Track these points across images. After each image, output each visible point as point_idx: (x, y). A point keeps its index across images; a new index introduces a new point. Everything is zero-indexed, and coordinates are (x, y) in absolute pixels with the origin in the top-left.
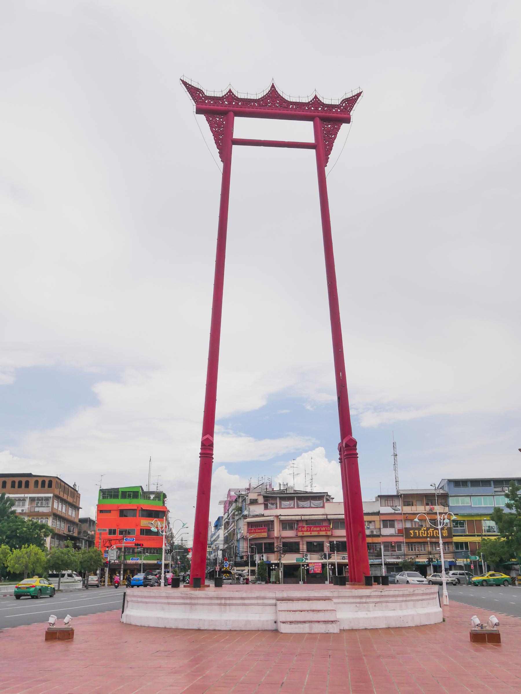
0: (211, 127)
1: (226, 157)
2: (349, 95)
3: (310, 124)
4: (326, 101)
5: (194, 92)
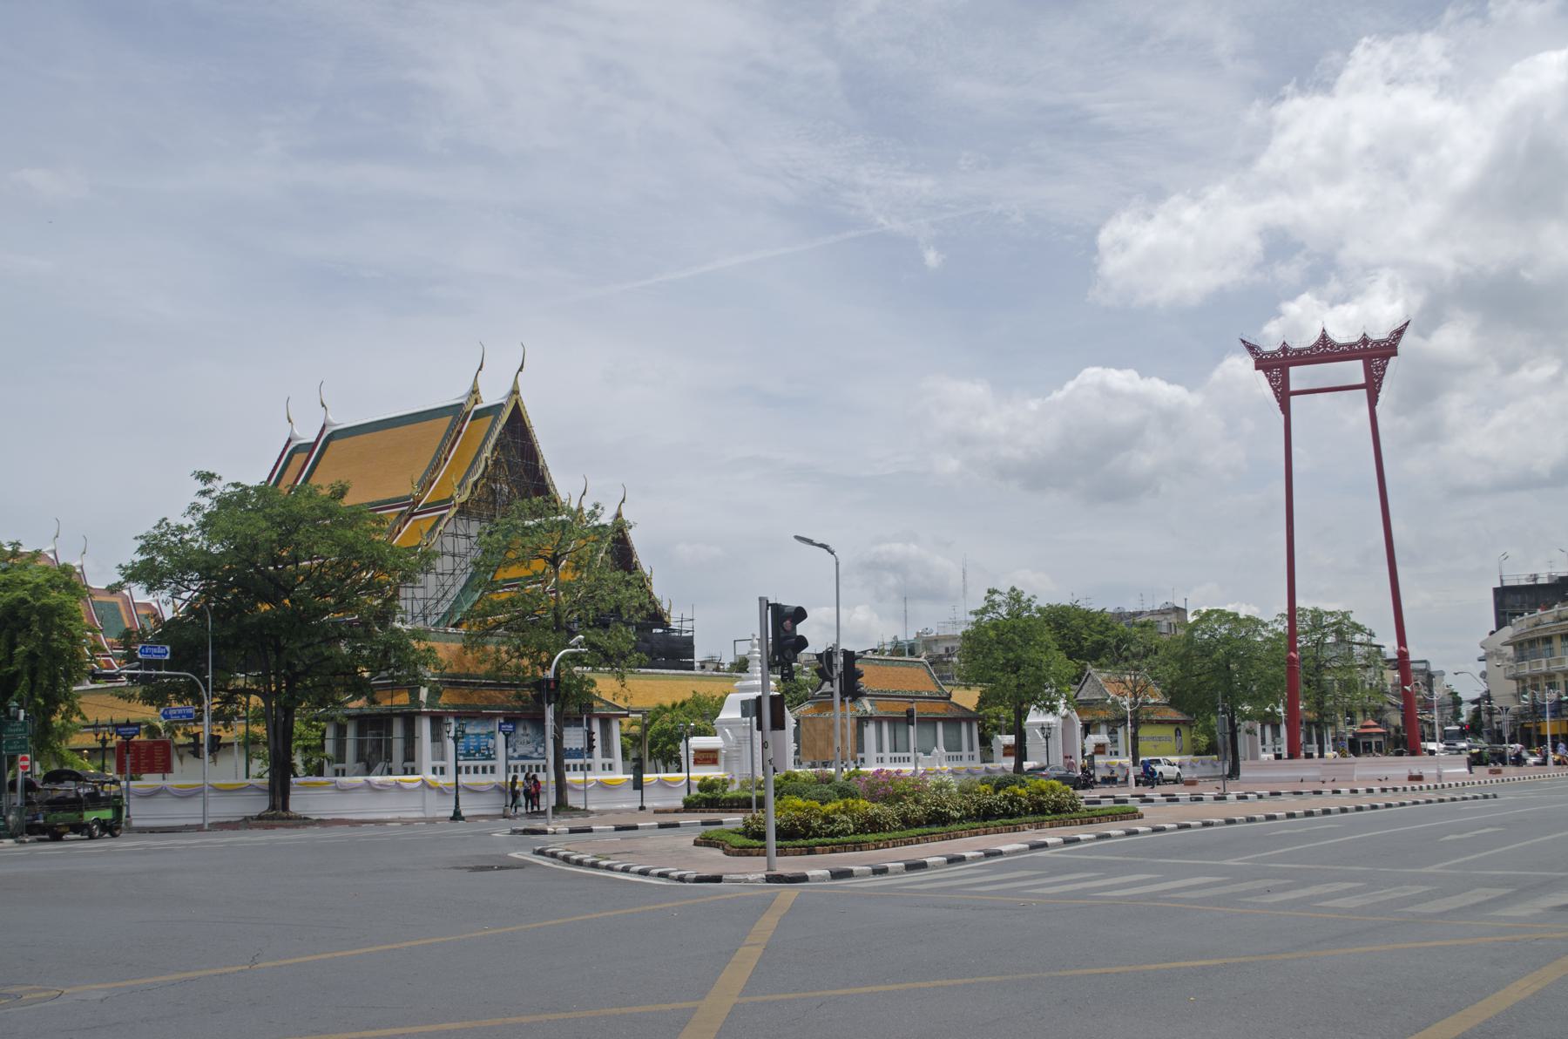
0: (1271, 381)
1: (1285, 408)
2: (1398, 326)
3: (1359, 363)
4: (1375, 337)
5: (1252, 349)
